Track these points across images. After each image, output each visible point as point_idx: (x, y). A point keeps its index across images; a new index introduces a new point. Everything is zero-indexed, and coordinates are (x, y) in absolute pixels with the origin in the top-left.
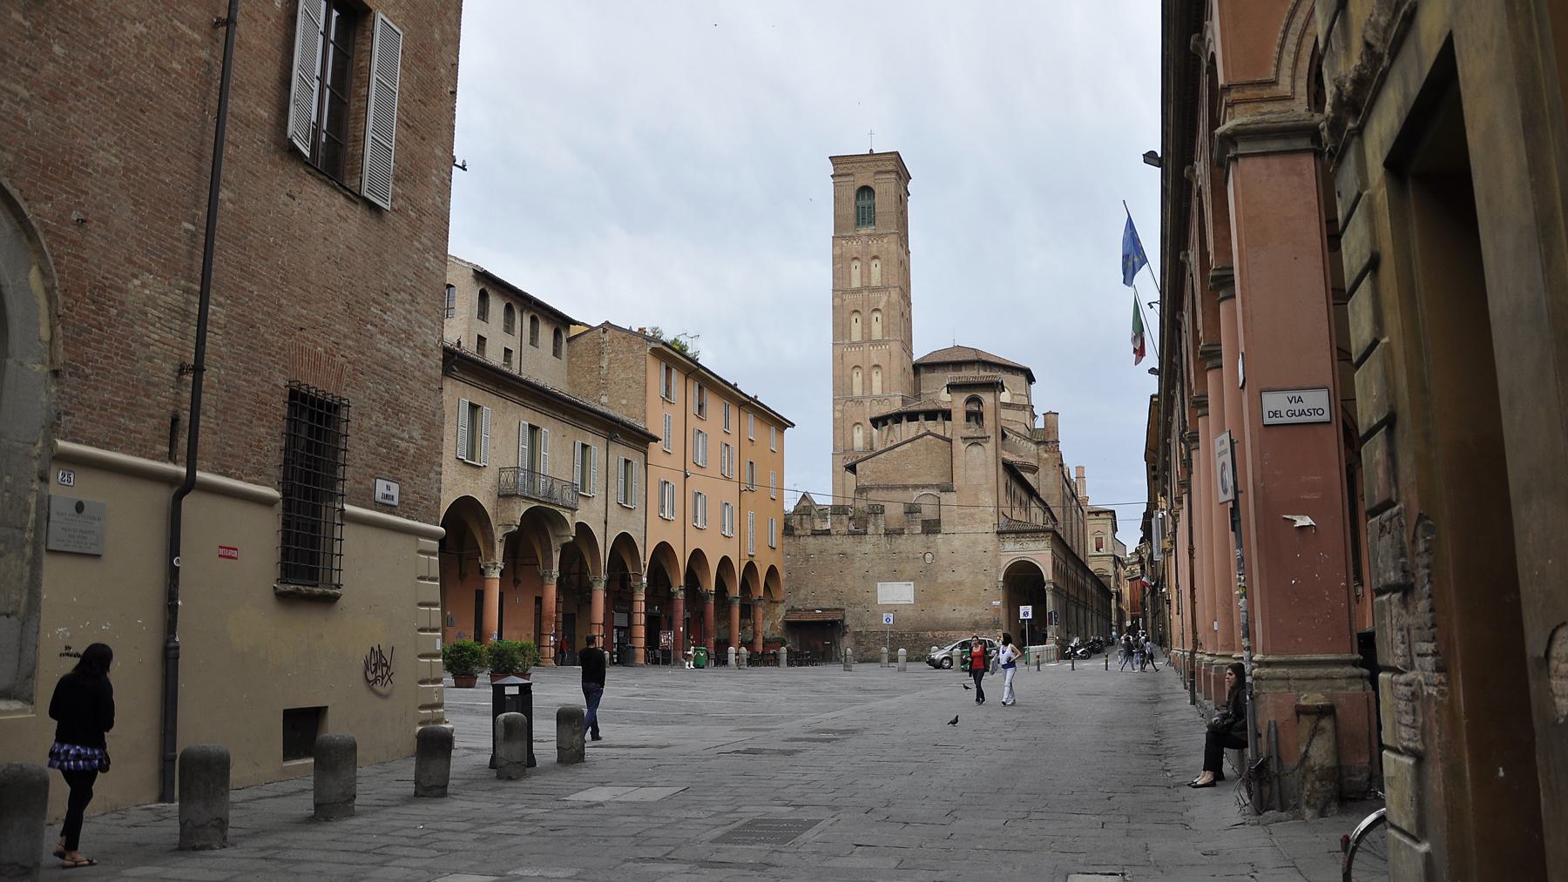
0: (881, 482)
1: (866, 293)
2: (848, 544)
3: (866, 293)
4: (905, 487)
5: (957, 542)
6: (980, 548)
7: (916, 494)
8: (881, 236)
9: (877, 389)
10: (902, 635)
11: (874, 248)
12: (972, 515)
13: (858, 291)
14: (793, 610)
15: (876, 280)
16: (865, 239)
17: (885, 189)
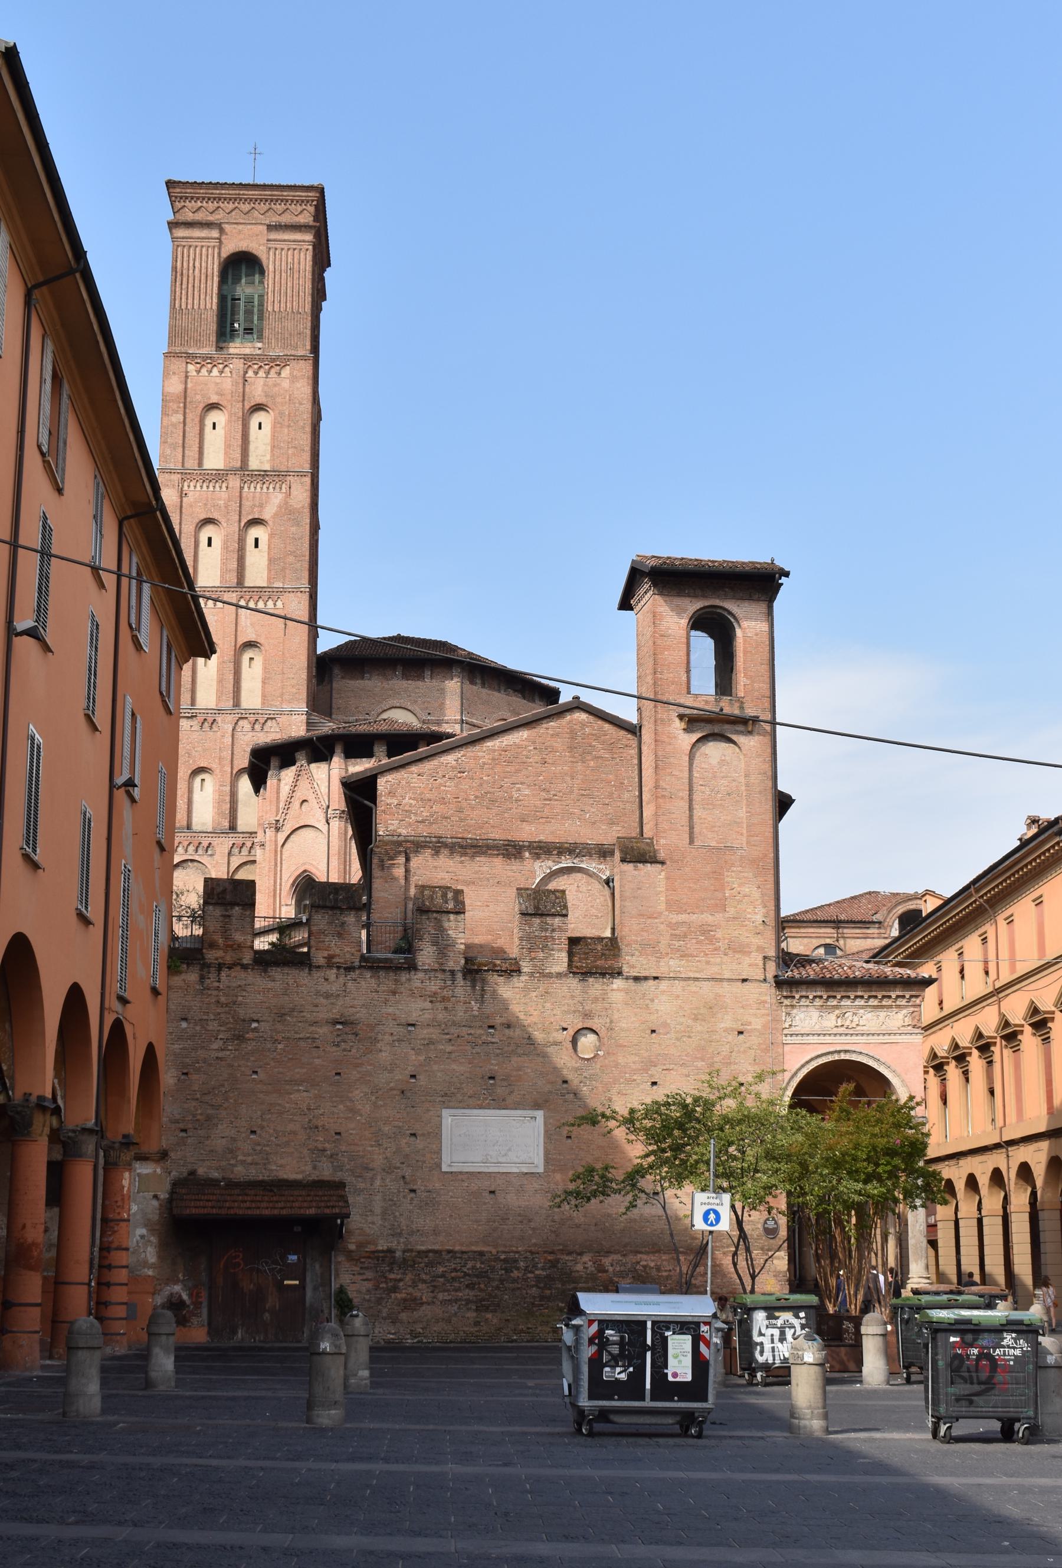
0: (445, 830)
1: (234, 482)
2: (361, 994)
3: (234, 482)
4: (512, 850)
5: (665, 1003)
6: (727, 1022)
7: (539, 869)
8: (277, 363)
9: (251, 698)
10: (510, 1264)
11: (257, 391)
12: (706, 931)
13: (219, 476)
14: (187, 1185)
15: (260, 458)
16: (237, 365)
17: (286, 262)
